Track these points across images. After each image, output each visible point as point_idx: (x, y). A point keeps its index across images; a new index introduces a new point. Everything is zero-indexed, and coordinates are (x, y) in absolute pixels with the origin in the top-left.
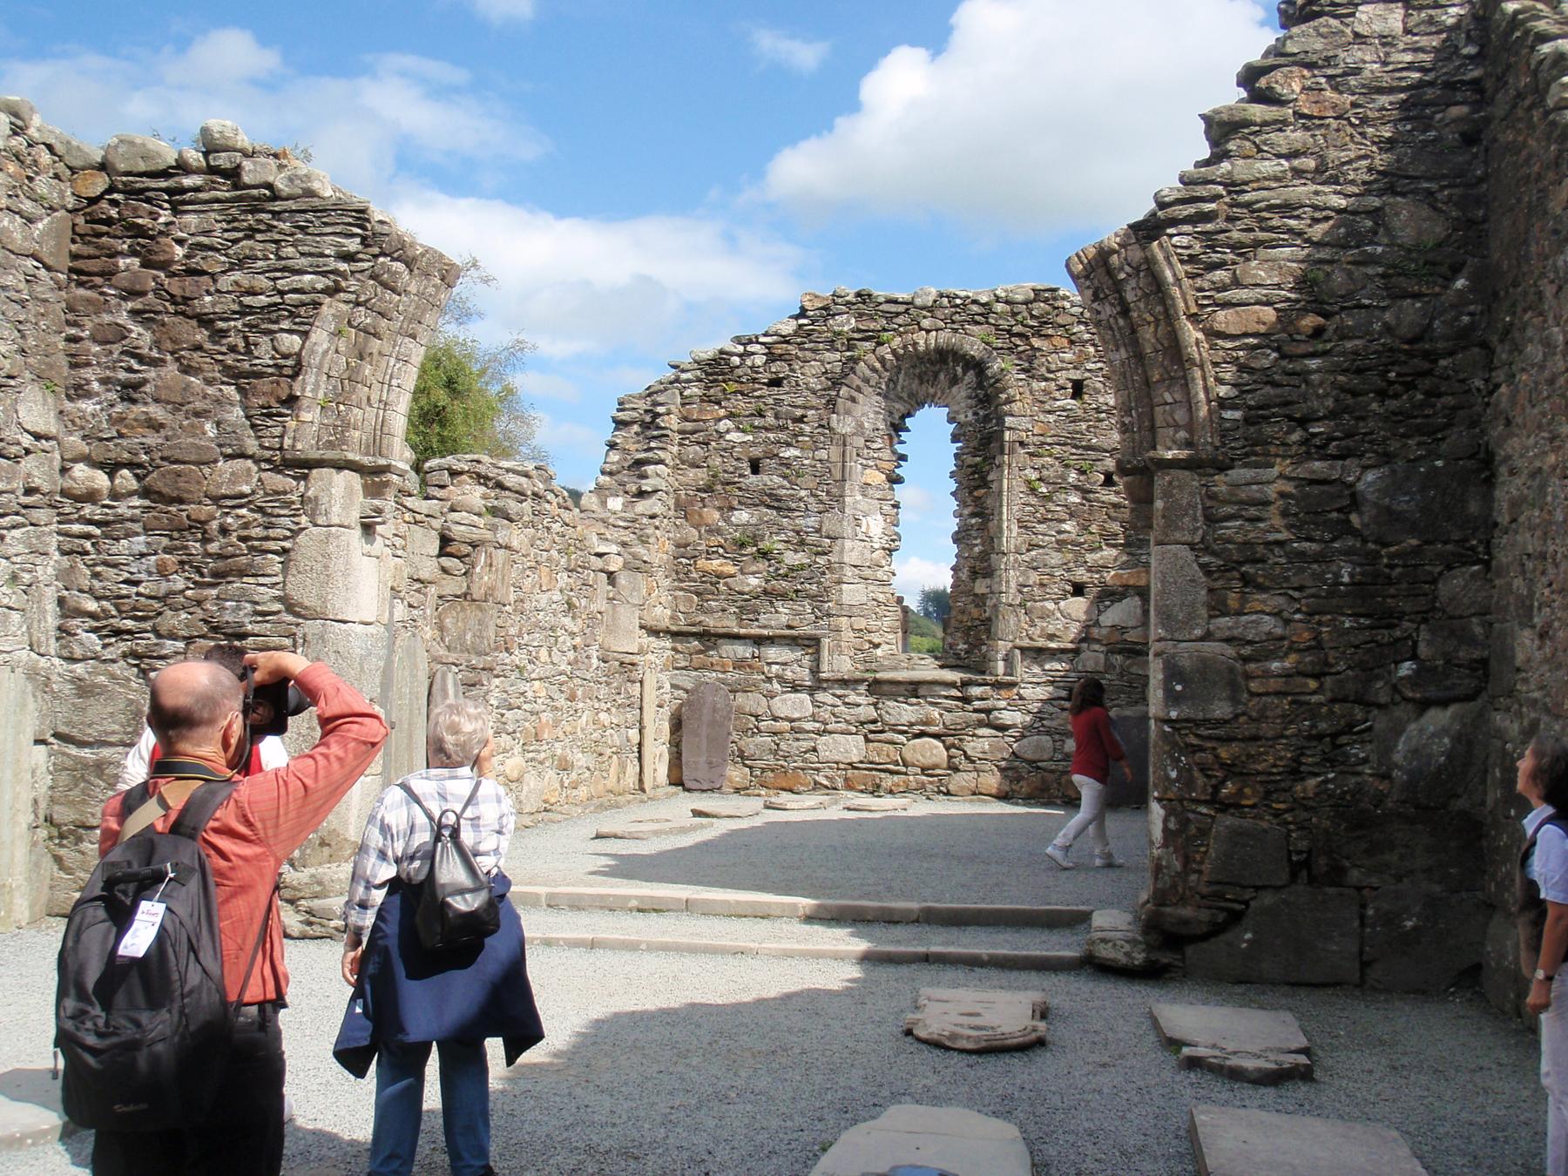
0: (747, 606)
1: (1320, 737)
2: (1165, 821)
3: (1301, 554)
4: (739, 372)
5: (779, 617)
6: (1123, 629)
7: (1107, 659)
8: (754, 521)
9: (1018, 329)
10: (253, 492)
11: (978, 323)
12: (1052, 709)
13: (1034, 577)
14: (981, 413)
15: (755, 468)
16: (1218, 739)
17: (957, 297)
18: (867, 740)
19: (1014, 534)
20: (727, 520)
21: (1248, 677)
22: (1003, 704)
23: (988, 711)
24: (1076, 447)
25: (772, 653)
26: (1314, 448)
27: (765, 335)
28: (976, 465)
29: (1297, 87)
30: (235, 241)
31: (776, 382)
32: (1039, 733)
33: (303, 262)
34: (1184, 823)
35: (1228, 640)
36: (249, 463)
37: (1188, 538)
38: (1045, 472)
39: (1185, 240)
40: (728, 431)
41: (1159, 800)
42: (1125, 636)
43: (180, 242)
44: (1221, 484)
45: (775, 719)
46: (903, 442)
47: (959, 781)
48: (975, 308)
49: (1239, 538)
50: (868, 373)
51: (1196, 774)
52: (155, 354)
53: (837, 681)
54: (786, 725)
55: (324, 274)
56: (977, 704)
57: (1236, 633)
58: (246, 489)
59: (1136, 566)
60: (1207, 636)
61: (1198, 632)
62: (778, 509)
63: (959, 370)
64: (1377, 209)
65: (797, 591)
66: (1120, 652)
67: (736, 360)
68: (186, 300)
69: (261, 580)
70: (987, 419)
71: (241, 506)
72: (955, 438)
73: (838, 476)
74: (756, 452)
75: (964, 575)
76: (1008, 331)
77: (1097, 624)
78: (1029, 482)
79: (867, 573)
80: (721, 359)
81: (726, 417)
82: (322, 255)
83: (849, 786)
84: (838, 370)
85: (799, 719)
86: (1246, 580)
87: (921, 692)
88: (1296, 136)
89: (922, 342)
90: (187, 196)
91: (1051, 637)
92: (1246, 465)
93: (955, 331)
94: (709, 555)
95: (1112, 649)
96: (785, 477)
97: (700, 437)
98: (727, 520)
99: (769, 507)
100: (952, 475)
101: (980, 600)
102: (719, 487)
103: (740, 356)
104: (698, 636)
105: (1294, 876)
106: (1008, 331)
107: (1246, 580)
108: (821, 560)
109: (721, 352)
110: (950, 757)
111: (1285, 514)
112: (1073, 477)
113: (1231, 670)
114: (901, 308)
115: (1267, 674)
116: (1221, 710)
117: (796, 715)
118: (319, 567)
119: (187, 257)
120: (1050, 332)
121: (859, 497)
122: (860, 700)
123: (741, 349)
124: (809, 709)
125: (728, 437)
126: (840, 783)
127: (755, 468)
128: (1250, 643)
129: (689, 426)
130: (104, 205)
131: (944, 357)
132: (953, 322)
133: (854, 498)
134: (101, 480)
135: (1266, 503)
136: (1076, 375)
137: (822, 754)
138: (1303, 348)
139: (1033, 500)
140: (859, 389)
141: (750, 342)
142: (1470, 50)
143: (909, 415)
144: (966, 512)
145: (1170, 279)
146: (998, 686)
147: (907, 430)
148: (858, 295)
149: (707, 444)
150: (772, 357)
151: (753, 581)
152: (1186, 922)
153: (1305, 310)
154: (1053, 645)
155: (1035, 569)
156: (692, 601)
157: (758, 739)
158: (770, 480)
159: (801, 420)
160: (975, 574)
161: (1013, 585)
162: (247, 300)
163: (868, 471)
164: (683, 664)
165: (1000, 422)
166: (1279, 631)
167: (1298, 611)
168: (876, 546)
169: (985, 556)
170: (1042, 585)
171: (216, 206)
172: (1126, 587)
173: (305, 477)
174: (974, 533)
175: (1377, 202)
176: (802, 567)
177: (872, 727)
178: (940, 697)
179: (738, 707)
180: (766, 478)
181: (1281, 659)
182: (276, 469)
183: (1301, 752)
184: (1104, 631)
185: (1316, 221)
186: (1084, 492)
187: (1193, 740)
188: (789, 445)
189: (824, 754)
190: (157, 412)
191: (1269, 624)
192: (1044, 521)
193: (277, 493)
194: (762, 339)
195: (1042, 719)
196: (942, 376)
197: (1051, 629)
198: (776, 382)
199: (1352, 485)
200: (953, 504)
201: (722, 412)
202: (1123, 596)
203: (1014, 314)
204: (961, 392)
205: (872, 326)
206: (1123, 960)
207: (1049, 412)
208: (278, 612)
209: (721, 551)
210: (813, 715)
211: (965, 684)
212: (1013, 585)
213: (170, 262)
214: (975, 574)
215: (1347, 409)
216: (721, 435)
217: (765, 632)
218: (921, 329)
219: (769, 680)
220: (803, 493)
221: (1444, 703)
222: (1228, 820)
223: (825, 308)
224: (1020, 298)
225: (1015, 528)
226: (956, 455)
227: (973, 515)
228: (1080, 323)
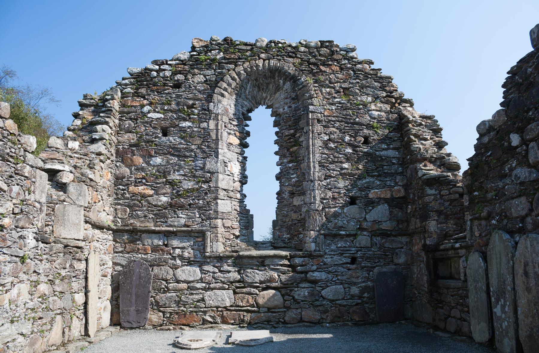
0: (160, 213)
4: (156, 80)
8: (164, 163)
9: (313, 60)
11: (291, 57)
12: (343, 270)
13: (330, 194)
14: (293, 106)
15: (165, 134)
17: (280, 43)
18: (235, 293)
19: (317, 170)
20: (148, 164)
23: (306, 272)
24: (348, 123)
27: (172, 60)
28: (291, 135)
31: (177, 85)
32: (336, 284)
38: (332, 136)
40: (149, 112)
42: (381, 226)
45: (178, 282)
46: (247, 125)
47: (291, 315)
48: (289, 49)
50: (231, 81)
53: (216, 257)
54: (185, 286)
59: (384, 187)
62: (178, 156)
63: (281, 81)
65: (190, 205)
67: (155, 74)
70: (297, 109)
72: (276, 124)
73: (214, 137)
74: (166, 124)
75: (286, 195)
79: (231, 194)
81: (147, 104)
83: (225, 321)
84: (214, 79)
85: (193, 282)
87: (267, 262)
89: (261, 65)
91: (341, 228)
93: (279, 60)
95: (374, 233)
96: (182, 138)
97: (132, 115)
98: (148, 164)
99: (173, 155)
100: (276, 142)
101: (299, 207)
103: (157, 71)
106: (308, 62)
108: (205, 186)
109: (146, 69)
110: (285, 301)
112: (347, 138)
117: (191, 279)
120: (330, 63)
121: (226, 150)
122: (230, 268)
123: (157, 67)
124: (199, 275)
125: (149, 115)
126: (219, 320)
129: (126, 110)
132: (277, 56)
133: (223, 150)
137: (207, 302)
139: (326, 151)
140: (225, 90)
141: (163, 63)
143: (250, 110)
144: (285, 161)
147: (250, 119)
148: (225, 40)
149: (136, 120)
150: (174, 73)
154: (343, 233)
155: (330, 189)
156: (125, 211)
157: (169, 295)
158: (173, 139)
159: (192, 106)
160: (292, 194)
161: (318, 198)
163: (231, 136)
164: (120, 249)
165: (306, 108)
168: (236, 179)
169: (298, 184)
172: (380, 199)
174: (291, 172)
176: (192, 190)
177: (238, 285)
178: (278, 265)
179: (155, 275)
180: (171, 138)
184: (370, 224)
186: (353, 147)
188: (185, 120)
189: (210, 302)
192: (333, 162)
194: (169, 62)
195: (337, 276)
196: (271, 86)
197: (340, 224)
198: (177, 85)
200: (277, 158)
201: (145, 102)
202: (378, 203)
203: (311, 53)
204: (281, 96)
207: (332, 104)
209: (144, 181)
210: (201, 279)
211: (292, 257)
212: (318, 198)
214: (292, 194)
217: (171, 229)
218: (260, 58)
219: (174, 258)
220: (193, 147)
223: (206, 46)
225: (317, 166)
226: (277, 133)
227: (290, 162)
228: (345, 59)
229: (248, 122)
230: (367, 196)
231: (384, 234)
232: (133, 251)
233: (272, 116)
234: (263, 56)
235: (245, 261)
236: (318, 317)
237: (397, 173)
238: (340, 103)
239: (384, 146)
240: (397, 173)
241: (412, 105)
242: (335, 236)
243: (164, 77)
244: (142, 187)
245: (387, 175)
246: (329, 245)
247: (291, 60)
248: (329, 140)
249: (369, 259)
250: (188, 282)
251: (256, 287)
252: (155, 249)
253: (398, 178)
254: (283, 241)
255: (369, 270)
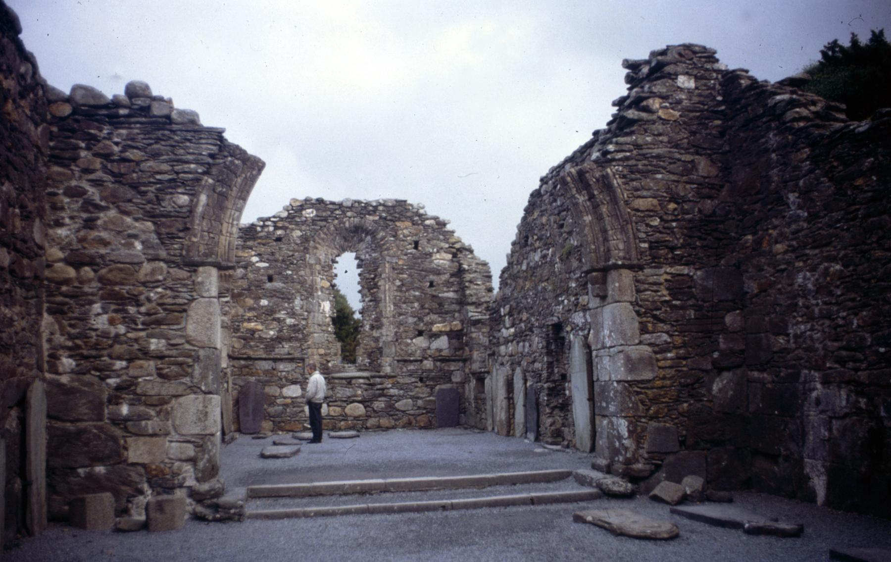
1: (687, 385)
2: (628, 427)
3: (675, 306)
5: (285, 348)
6: (441, 351)
7: (434, 364)
9: (389, 218)
10: (165, 279)
11: (370, 215)
16: (648, 388)
21: (658, 360)
22: (390, 386)
23: (383, 389)
25: (281, 366)
26: (677, 261)
29: (657, 106)
30: (150, 145)
31: (279, 239)
32: (407, 398)
33: (190, 157)
34: (636, 426)
35: (650, 345)
36: (162, 264)
37: (630, 299)
39: (621, 168)
41: (625, 417)
43: (117, 144)
44: (641, 275)
47: (371, 422)
49: (651, 299)
51: (640, 404)
52: (103, 204)
55: (202, 164)
56: (379, 387)
57: (653, 341)
58: (160, 278)
60: (640, 343)
61: (637, 341)
62: (283, 298)
64: (693, 161)
66: (440, 360)
68: (122, 175)
69: (172, 327)
71: (157, 287)
72: (359, 266)
76: (385, 219)
77: (429, 348)
78: (399, 287)
79: (324, 328)
80: (252, 227)
82: (201, 154)
86: (655, 317)
87: (353, 381)
88: (659, 127)
90: (122, 119)
91: (410, 355)
92: (652, 267)
94: (249, 320)
95: (435, 360)
100: (359, 283)
101: (377, 340)
102: (253, 288)
104: (245, 359)
105: (681, 446)
107: (655, 317)
111: (667, 289)
113: (651, 358)
114: (337, 207)
115: (665, 359)
116: (648, 375)
117: (294, 395)
118: (205, 319)
119: (121, 152)
123: (261, 223)
125: (257, 265)
127: (270, 279)
128: (658, 345)
130: (70, 121)
131: (358, 230)
134: (71, 272)
135: (661, 284)
136: (415, 238)
138: (670, 218)
142: (719, 98)
143: (339, 255)
144: (367, 299)
145: (616, 185)
146: (387, 377)
147: (337, 262)
150: (276, 228)
151: (272, 333)
152: (641, 471)
153: (670, 201)
157: (276, 408)
158: (278, 284)
162: (158, 177)
166: (669, 340)
167: (676, 331)
169: (377, 320)
170: (405, 332)
171: (138, 125)
172: (441, 332)
173: (195, 271)
175: (689, 158)
181: (670, 351)
182: (178, 266)
183: (680, 391)
185: (670, 163)
187: (636, 389)
190: (104, 235)
191: (665, 337)
192: (404, 303)
193: (179, 279)
199: (692, 277)
200: (359, 296)
201: (253, 253)
204: (362, 246)
205: (324, 214)
206: (622, 489)
207: (406, 255)
208: (183, 344)
213: (112, 154)
215: (689, 245)
216: (254, 264)
221: (728, 369)
222: (654, 424)
224: (390, 204)
226: (360, 275)
227: (371, 301)
229: (335, 265)
230: (431, 330)
231: (445, 360)
232: (248, 374)
233: (356, 258)
234: (349, 214)
235: (337, 381)
236: (393, 423)
237: (455, 311)
238: (411, 253)
239: (445, 289)
240: (455, 311)
241: (471, 251)
242: (405, 361)
243: (268, 232)
244: (253, 324)
245: (447, 313)
246: (401, 368)
247: (371, 218)
248: (403, 285)
249: (433, 379)
250: (292, 398)
251: (345, 401)
252: (266, 372)
253: (457, 315)
254: (365, 365)
255: (432, 388)
